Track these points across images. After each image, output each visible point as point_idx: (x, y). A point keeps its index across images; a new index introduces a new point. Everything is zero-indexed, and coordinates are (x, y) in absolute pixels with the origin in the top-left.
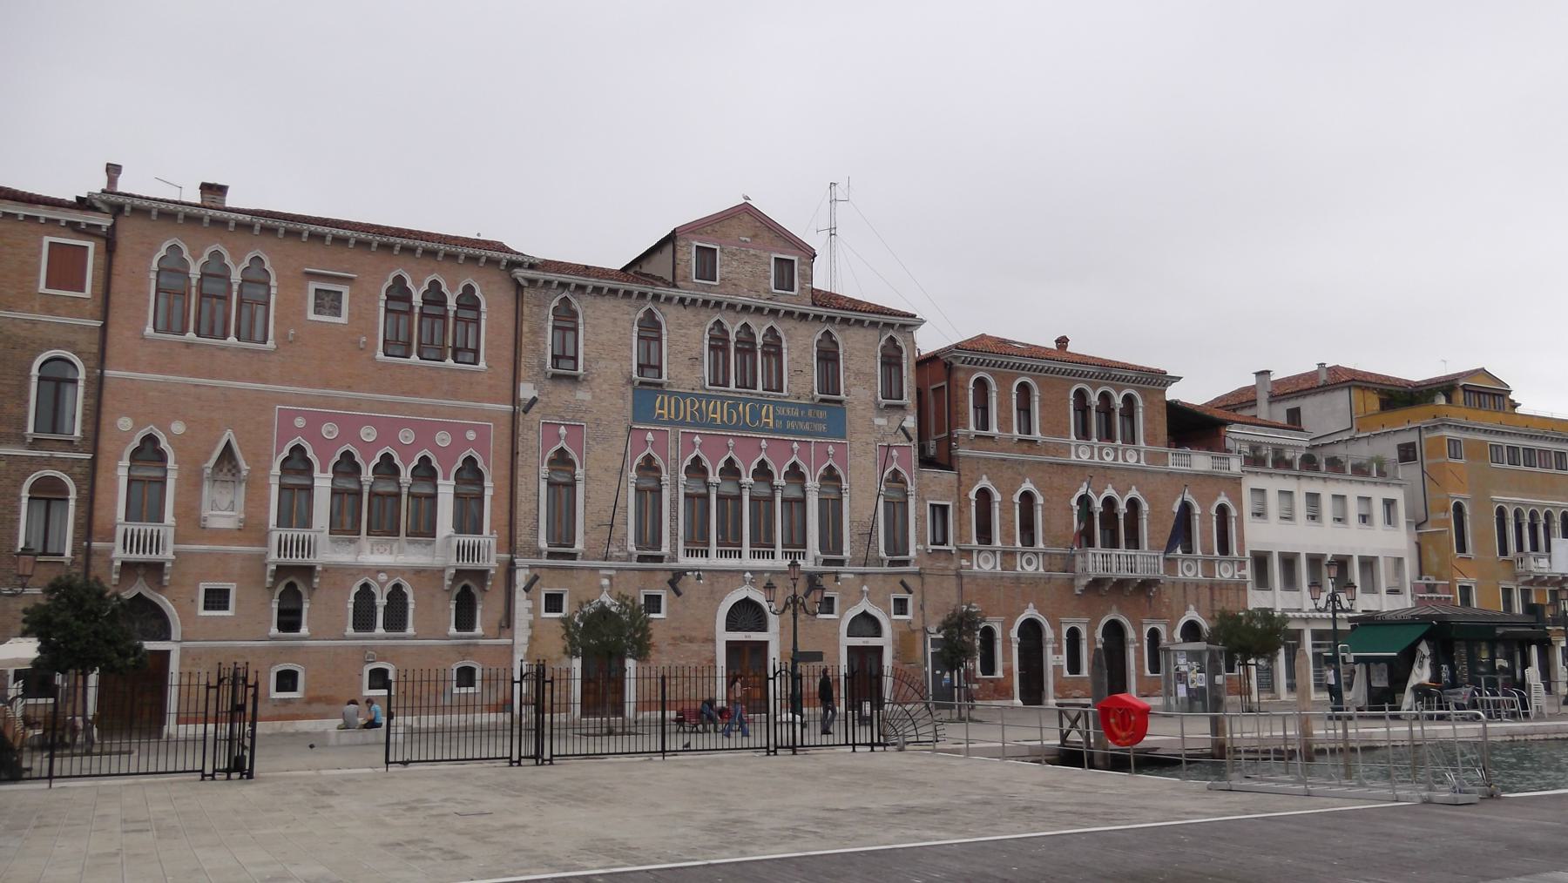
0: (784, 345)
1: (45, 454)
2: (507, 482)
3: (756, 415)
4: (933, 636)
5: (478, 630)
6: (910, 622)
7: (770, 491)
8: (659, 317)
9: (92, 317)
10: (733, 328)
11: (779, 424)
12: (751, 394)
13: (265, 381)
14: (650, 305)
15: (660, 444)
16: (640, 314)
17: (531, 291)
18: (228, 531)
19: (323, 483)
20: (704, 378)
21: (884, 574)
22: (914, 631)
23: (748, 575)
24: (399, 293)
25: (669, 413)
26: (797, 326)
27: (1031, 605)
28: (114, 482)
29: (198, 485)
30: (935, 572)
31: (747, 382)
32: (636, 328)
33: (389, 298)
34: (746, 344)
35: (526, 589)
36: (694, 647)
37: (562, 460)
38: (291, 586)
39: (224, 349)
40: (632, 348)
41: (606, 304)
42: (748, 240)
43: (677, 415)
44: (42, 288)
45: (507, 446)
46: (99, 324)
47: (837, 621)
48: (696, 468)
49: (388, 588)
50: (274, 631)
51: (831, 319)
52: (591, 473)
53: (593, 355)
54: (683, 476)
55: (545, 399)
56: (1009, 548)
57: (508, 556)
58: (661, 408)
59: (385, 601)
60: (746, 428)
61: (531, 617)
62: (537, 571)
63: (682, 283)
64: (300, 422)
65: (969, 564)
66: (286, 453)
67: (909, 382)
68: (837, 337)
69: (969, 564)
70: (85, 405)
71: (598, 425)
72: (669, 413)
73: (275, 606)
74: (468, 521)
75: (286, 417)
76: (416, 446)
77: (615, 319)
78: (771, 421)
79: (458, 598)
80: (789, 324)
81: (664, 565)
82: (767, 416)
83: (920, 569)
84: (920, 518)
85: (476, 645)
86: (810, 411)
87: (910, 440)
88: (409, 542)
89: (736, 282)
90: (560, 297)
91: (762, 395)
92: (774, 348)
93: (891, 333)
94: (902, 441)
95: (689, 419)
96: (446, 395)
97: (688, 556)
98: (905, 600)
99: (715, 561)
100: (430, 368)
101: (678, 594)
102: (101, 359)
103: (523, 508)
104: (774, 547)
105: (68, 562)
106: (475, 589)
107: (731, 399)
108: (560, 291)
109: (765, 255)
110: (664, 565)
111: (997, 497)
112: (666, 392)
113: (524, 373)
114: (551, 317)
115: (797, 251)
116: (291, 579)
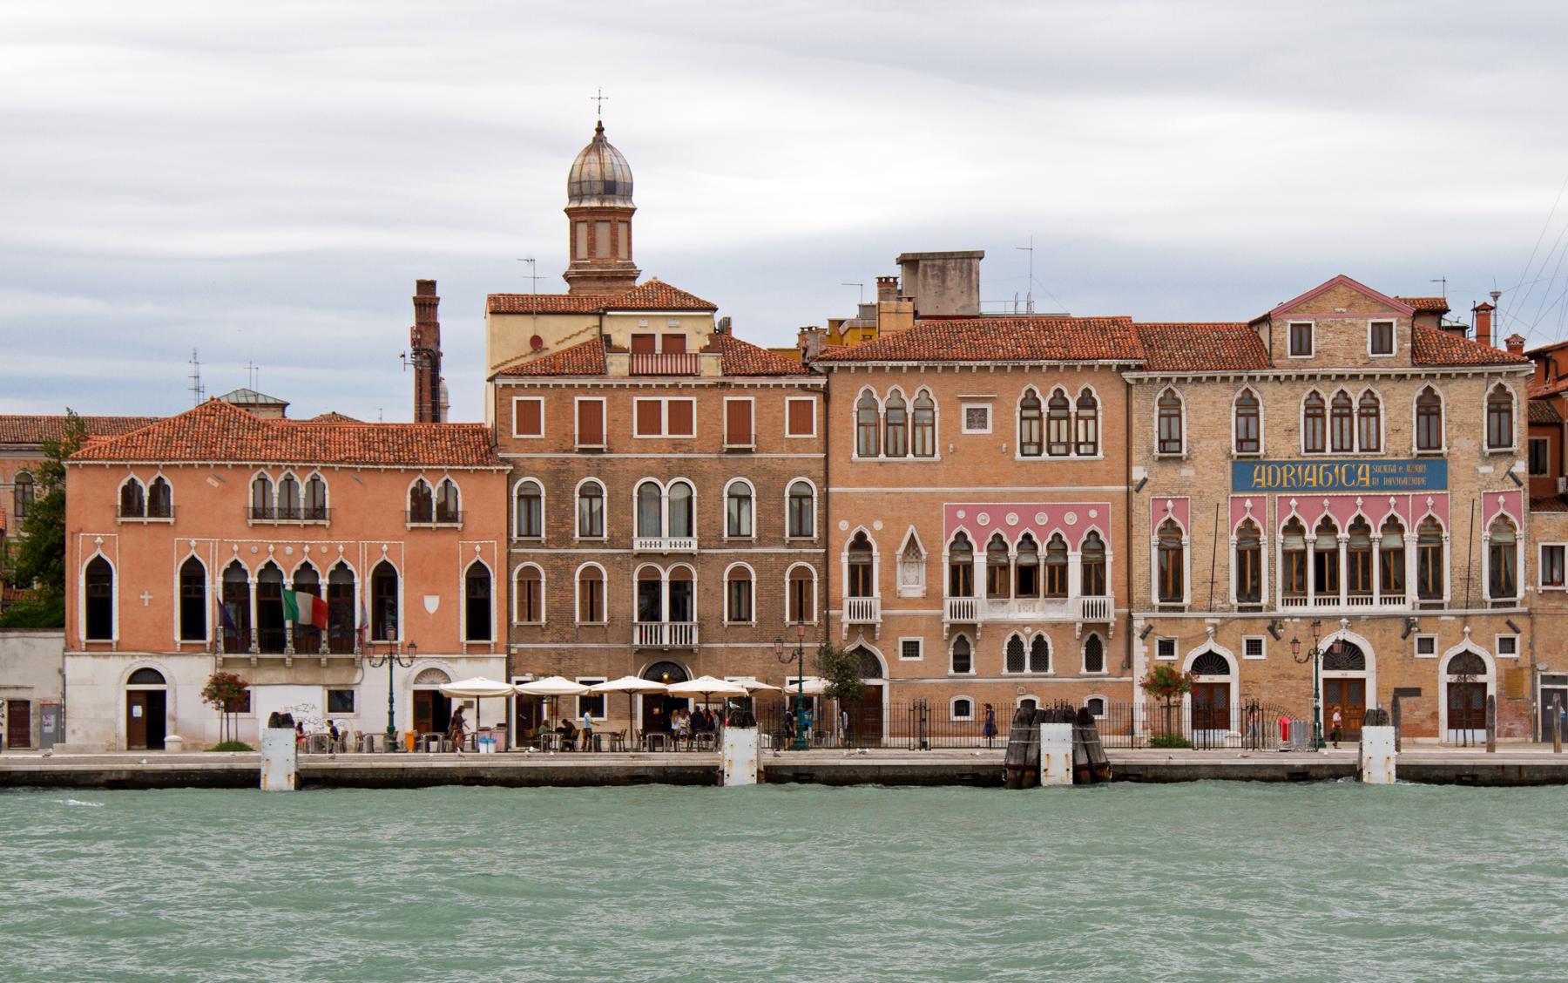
0: (1382, 406)
1: (797, 551)
2: (1125, 550)
3: (1351, 475)
4: (1544, 673)
5: (1105, 670)
6: (1517, 661)
8: (1256, 395)
9: (819, 451)
10: (1328, 397)
11: (1376, 481)
13: (935, 485)
14: (1247, 386)
15: (1258, 509)
16: (1239, 394)
17: (1139, 387)
18: (915, 599)
20: (1300, 446)
21: (1488, 615)
22: (1521, 669)
23: (1344, 621)
24: (1031, 403)
25: (1267, 481)
26: (1395, 386)
28: (840, 567)
29: (894, 568)
30: (1548, 611)
32: (1234, 408)
33: (1023, 408)
34: (1342, 408)
35: (1143, 637)
36: (1293, 683)
37: (1170, 531)
38: (962, 638)
39: (905, 464)
40: (1230, 427)
41: (1206, 391)
42: (1344, 310)
43: (1274, 481)
44: (787, 435)
45: (1123, 520)
46: (823, 455)
47: (1437, 660)
48: (1294, 528)
49: (1032, 639)
50: (951, 671)
51: (1432, 376)
52: (1196, 539)
54: (1280, 536)
55: (1154, 479)
57: (1126, 610)
58: (1259, 476)
59: (1031, 649)
60: (1342, 488)
61: (1147, 659)
62: (1151, 622)
63: (1278, 361)
64: (961, 514)
66: (952, 538)
67: (1519, 427)
68: (1438, 391)
70: (818, 515)
71: (1201, 497)
72: (1267, 481)
73: (951, 653)
74: (1094, 581)
75: (952, 511)
77: (1214, 402)
78: (1367, 480)
79: (1088, 645)
80: (1387, 386)
81: (1263, 614)
82: (1364, 475)
83: (1529, 609)
84: (1530, 560)
85: (1104, 682)
86: (1408, 467)
87: (1520, 484)
88: (1048, 602)
89: (1331, 352)
91: (1358, 456)
92: (1371, 409)
93: (1499, 380)
94: (1511, 486)
95: (1285, 484)
96: (1071, 483)
98: (1513, 640)
99: (1311, 609)
100: (1058, 462)
101: (1278, 638)
102: (827, 481)
103: (1138, 570)
104: (1372, 593)
105: (816, 625)
106: (1101, 638)
107: (1326, 462)
109: (1360, 322)
110: (1263, 614)
112: (1262, 463)
113: (1135, 458)
114: (1157, 408)
115: (1396, 313)
116: (962, 633)
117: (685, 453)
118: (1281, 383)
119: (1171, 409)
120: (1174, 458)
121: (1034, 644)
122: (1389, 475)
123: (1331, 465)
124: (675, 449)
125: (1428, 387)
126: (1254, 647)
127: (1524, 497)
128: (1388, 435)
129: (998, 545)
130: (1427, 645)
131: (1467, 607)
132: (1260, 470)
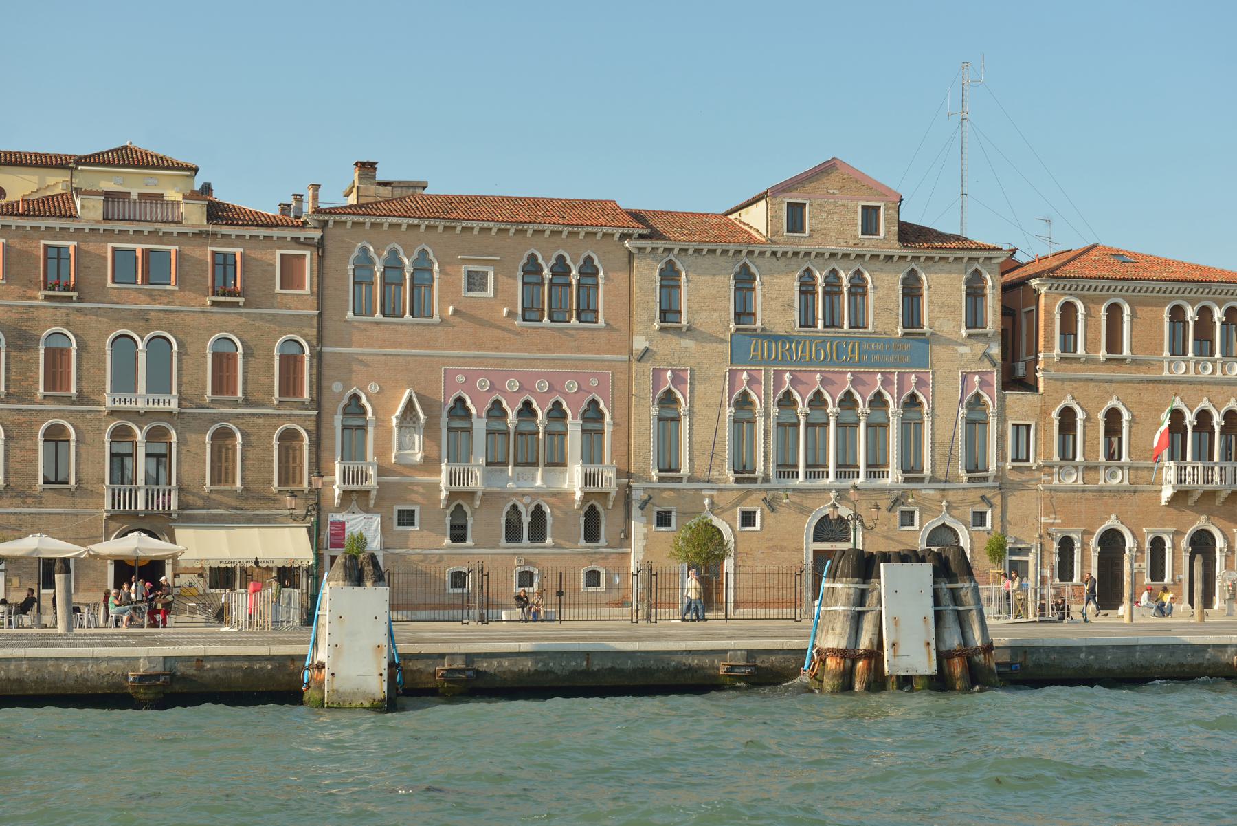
1: (287, 412)
5: (603, 541)
7: (856, 418)
9: (311, 308)
12: (839, 332)
16: (737, 268)
19: (480, 426)
20: (794, 321)
27: (1113, 516)
28: (333, 431)
33: (526, 272)
36: (785, 554)
38: (459, 507)
39: (402, 324)
40: (729, 299)
43: (769, 355)
44: (278, 289)
46: (316, 312)
48: (787, 401)
49: (531, 508)
50: (448, 541)
51: (917, 258)
54: (774, 410)
56: (1092, 463)
59: (529, 519)
60: (835, 365)
62: (650, 492)
64: (460, 379)
79: (586, 515)
81: (758, 485)
87: (995, 365)
89: (825, 232)
91: (848, 333)
92: (858, 289)
94: (986, 366)
97: (780, 477)
104: (859, 468)
106: (600, 508)
108: (666, 254)
109: (851, 204)
111: (1080, 415)
117: (164, 304)
118: (777, 259)
119: (670, 276)
120: (675, 328)
121: (533, 514)
122: (877, 352)
123: (823, 341)
124: (154, 300)
125: (913, 270)
126: (748, 518)
127: (995, 379)
128: (876, 314)
129: (497, 411)
132: (756, 344)
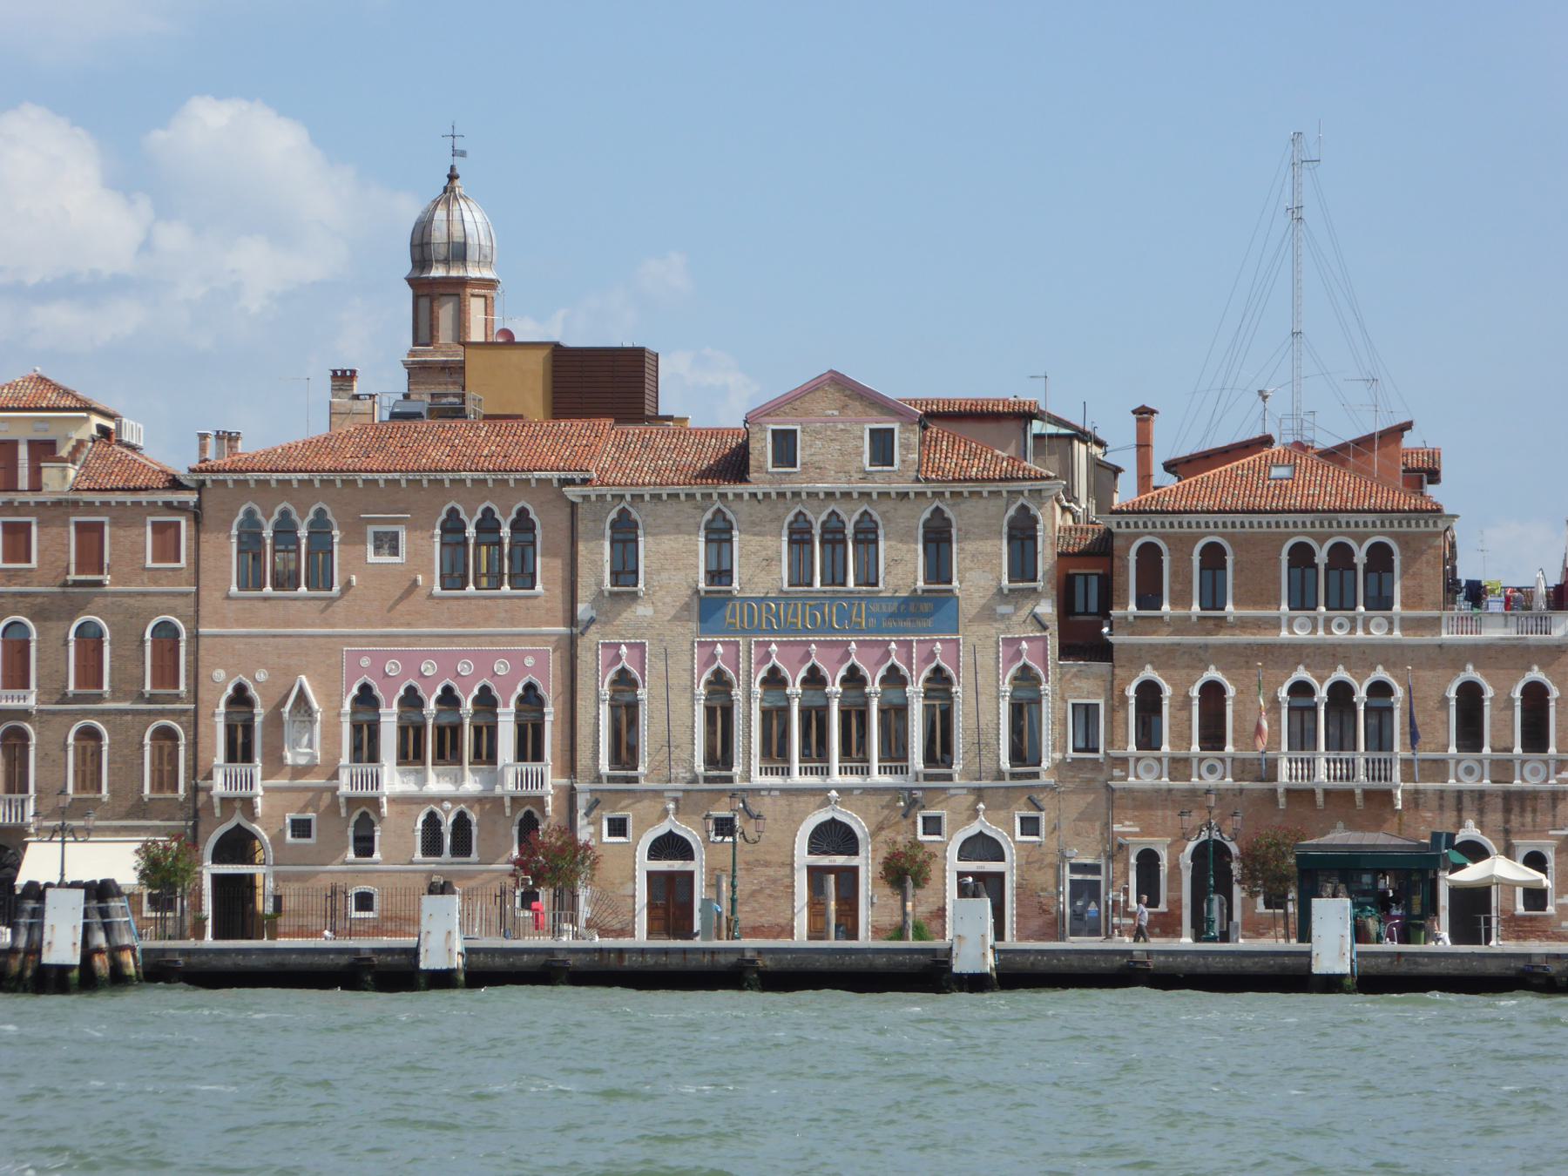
10: (817, 519)
17: (586, 506)
21: (1007, 788)
23: (834, 793)
25: (742, 621)
28: (213, 728)
31: (835, 576)
35: (587, 814)
37: (624, 681)
40: (697, 555)
42: (836, 413)
46: (194, 589)
47: (945, 845)
48: (774, 680)
50: (351, 855)
51: (938, 495)
53: (654, 566)
56: (1182, 753)
60: (833, 631)
62: (598, 795)
63: (756, 475)
64: (365, 662)
65: (1123, 774)
66: (355, 691)
69: (1123, 774)
70: (187, 662)
72: (742, 621)
74: (529, 747)
76: (476, 676)
80: (886, 505)
90: (617, 509)
91: (851, 592)
96: (502, 623)
98: (1037, 819)
102: (195, 620)
103: (583, 731)
105: (181, 799)
109: (857, 427)
116: (363, 809)
127: (1053, 643)
130: (933, 825)
131: (980, 779)
